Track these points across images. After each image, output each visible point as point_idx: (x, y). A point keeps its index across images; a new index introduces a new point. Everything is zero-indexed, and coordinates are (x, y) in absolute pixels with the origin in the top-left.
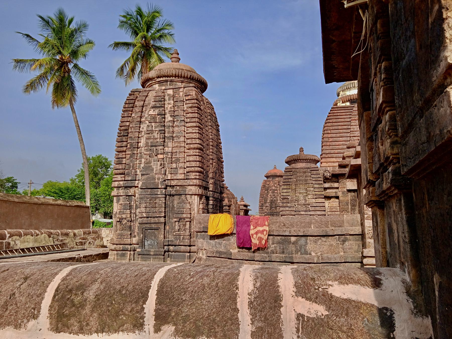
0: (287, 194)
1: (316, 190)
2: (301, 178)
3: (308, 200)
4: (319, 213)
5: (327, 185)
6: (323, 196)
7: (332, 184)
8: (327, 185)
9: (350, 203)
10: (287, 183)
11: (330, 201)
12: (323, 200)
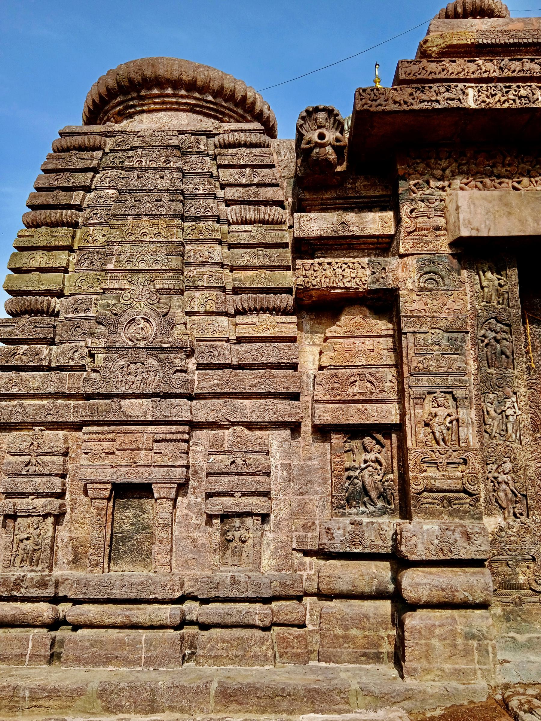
0: (51, 281)
1: (241, 257)
2: (151, 180)
3: (180, 317)
4: (251, 410)
5: (317, 224)
6: (288, 300)
7: (351, 217)
8: (317, 224)
10: (56, 215)
11: (333, 330)
12: (287, 325)
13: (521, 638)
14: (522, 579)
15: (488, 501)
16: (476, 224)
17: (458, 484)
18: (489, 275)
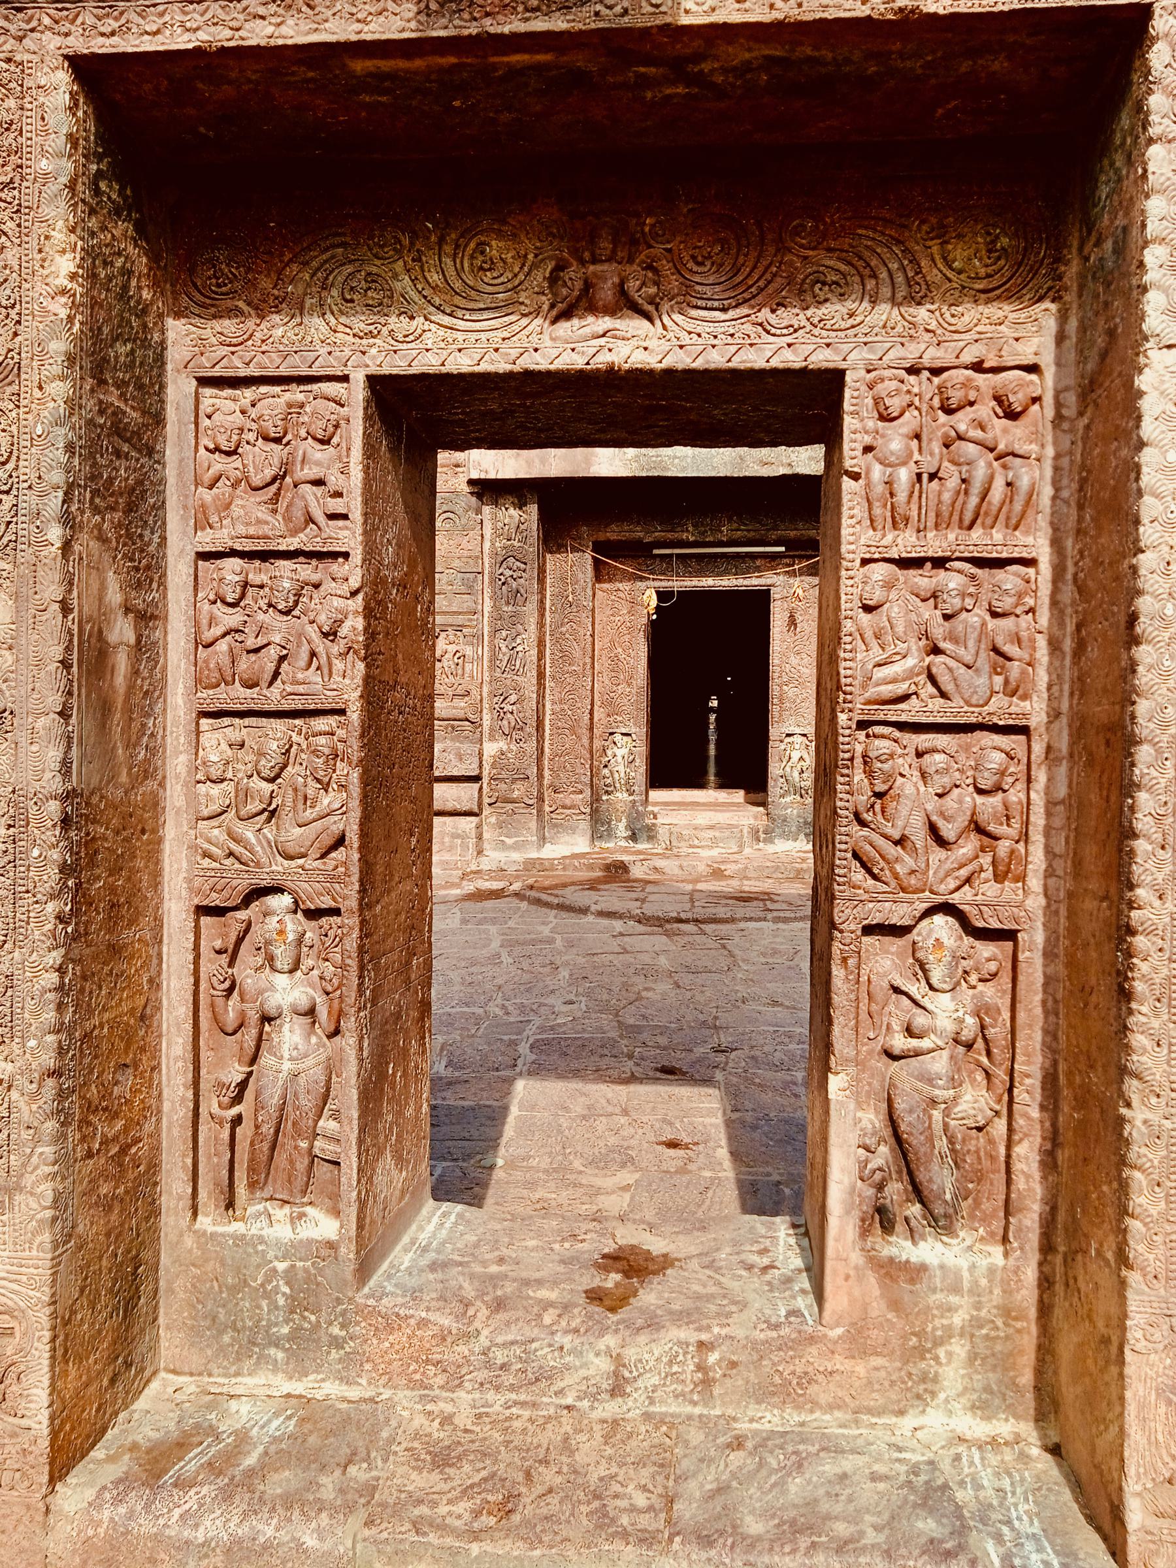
9: (493, 581)
13: (509, 841)
14: (516, 794)
15: (491, 729)
16: (484, 466)
17: (461, 714)
18: (512, 511)
